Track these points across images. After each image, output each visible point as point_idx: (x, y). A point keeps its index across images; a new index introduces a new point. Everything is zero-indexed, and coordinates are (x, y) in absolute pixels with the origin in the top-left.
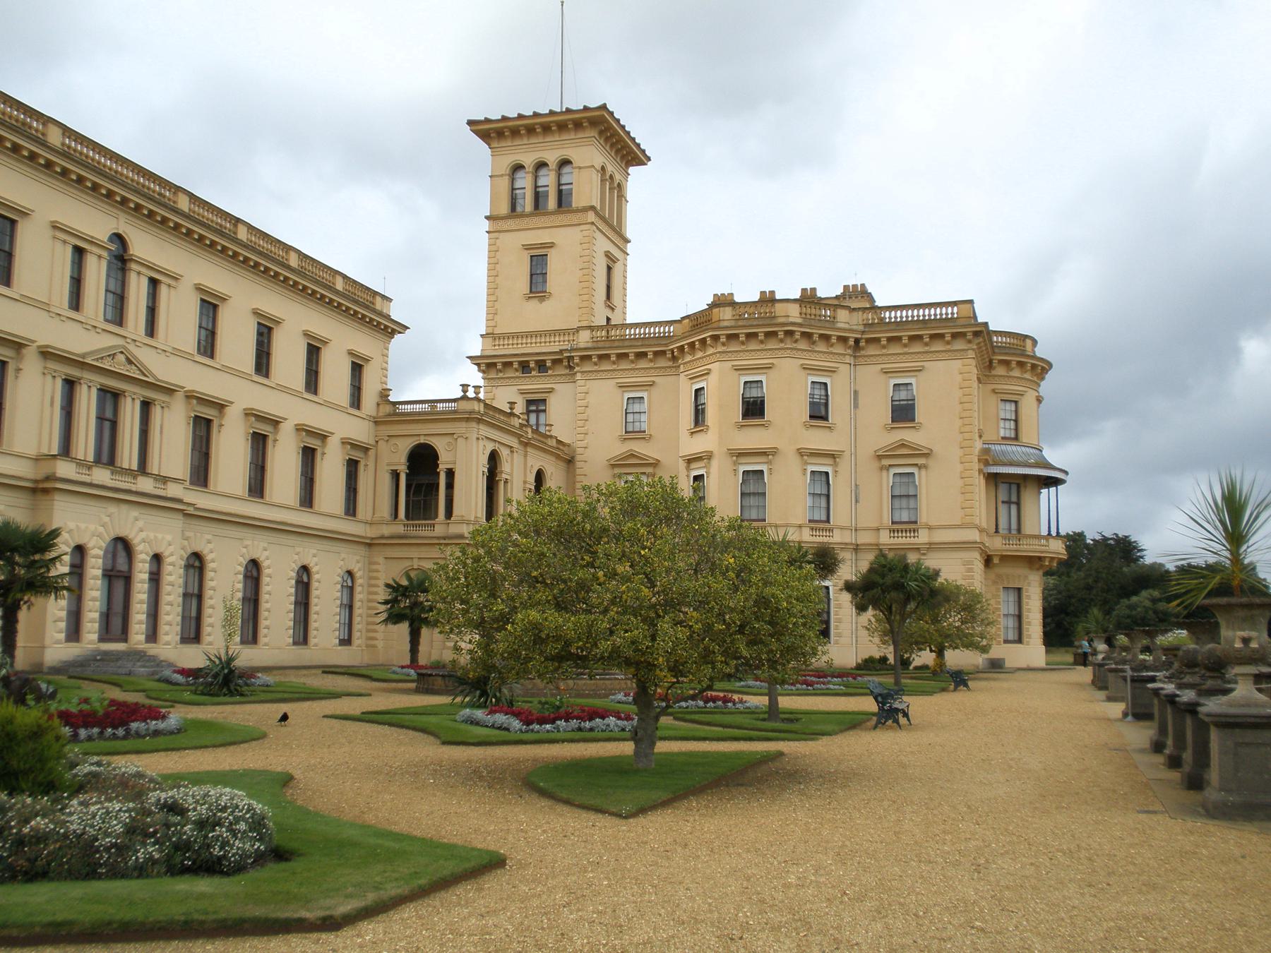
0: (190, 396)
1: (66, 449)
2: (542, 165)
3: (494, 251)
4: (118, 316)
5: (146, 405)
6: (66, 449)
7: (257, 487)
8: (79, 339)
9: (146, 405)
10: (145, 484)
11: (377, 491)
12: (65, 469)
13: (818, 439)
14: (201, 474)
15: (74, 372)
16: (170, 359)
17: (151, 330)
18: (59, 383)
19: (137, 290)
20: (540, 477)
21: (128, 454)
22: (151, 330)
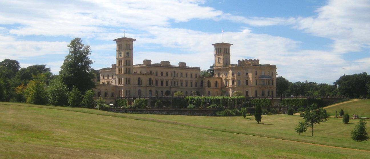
2: (219, 49)
3: (215, 58)
4: (175, 76)
5: (177, 82)
7: (187, 86)
8: (172, 78)
9: (177, 82)
10: (177, 87)
11: (199, 85)
12: (172, 87)
13: (239, 77)
14: (182, 85)
16: (179, 78)
17: (177, 76)
19: (176, 74)
20: (216, 82)
21: (176, 85)
22: (177, 76)
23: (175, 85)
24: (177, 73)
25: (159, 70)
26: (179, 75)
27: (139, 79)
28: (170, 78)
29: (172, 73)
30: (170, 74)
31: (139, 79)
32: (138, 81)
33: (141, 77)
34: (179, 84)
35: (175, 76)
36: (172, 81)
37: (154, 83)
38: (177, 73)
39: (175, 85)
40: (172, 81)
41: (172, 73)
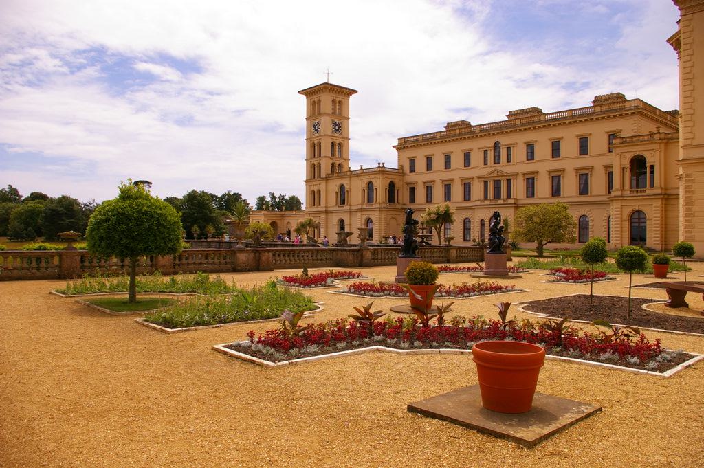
0: (524, 174)
1: (486, 198)
4: (497, 160)
5: (509, 182)
6: (486, 198)
8: (485, 171)
9: (509, 182)
15: (485, 180)
16: (518, 165)
17: (509, 160)
18: (483, 183)
22: (509, 160)
23: (497, 196)
24: (509, 149)
25: (438, 153)
26: (519, 153)
27: (342, 187)
28: (479, 169)
29: (486, 152)
30: (477, 158)
31: (342, 187)
32: (339, 194)
33: (345, 182)
34: (519, 189)
35: (497, 160)
36: (486, 183)
37: (381, 195)
38: (509, 149)
39: (497, 196)
40: (486, 183)
41: (486, 152)
